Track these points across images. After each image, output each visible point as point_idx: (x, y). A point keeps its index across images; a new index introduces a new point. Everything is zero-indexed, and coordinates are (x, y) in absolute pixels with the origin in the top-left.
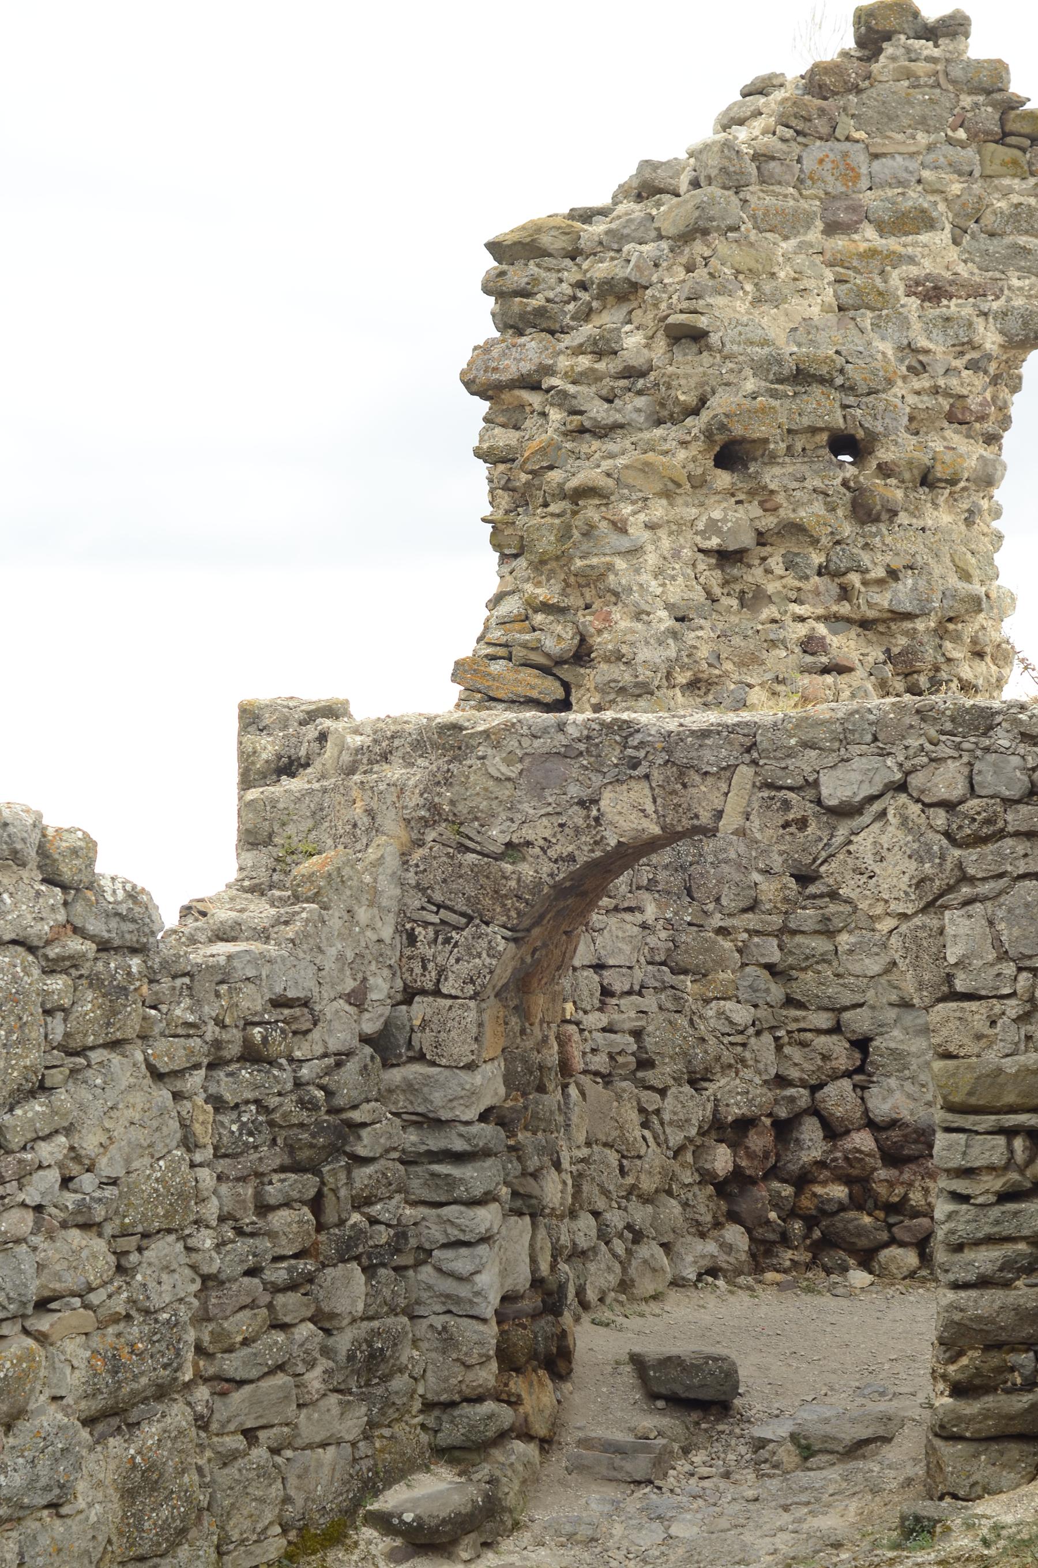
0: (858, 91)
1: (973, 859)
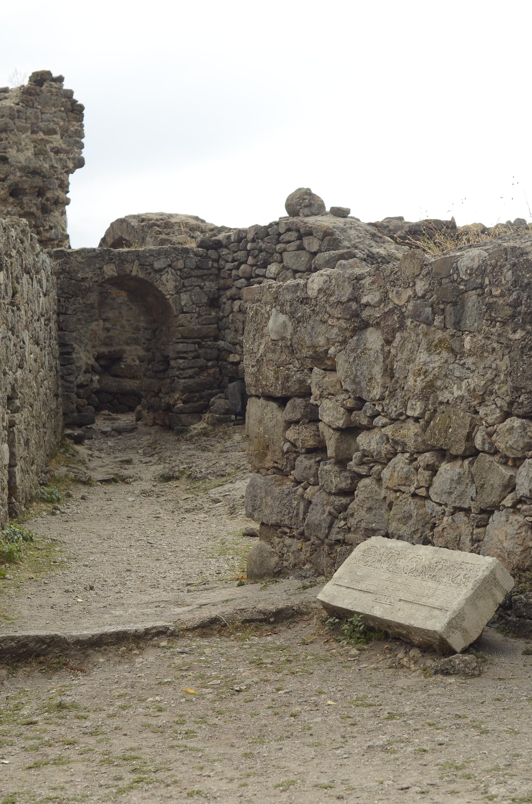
0: (38, 95)
1: (186, 282)
